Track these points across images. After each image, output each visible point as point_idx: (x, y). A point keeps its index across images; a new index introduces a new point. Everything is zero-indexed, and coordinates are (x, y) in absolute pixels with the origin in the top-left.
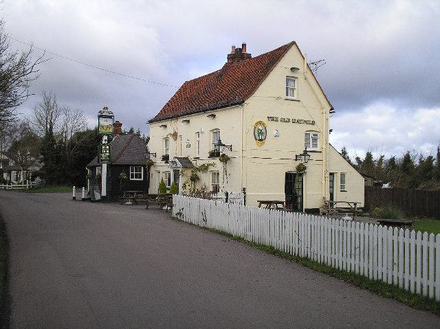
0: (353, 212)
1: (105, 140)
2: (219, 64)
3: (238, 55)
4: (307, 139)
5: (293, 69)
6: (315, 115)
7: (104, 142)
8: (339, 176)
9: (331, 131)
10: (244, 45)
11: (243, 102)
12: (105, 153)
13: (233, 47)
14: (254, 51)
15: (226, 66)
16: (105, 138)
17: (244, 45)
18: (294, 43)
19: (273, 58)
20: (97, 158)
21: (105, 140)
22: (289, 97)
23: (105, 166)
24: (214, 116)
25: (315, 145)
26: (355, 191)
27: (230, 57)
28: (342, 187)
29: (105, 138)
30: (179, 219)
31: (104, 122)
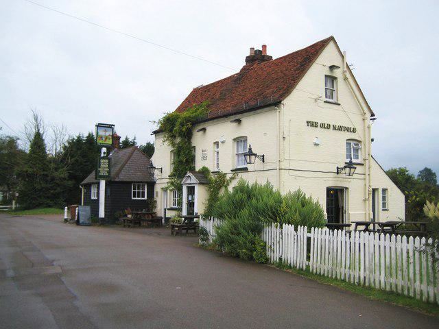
0: (392, 229)
1: (104, 153)
2: (235, 65)
3: (257, 58)
4: (349, 150)
5: (332, 68)
6: (353, 120)
7: (102, 155)
8: (380, 191)
9: (372, 140)
10: (264, 47)
11: (280, 102)
12: (104, 167)
13: (252, 49)
14: (275, 52)
15: (244, 69)
16: (104, 150)
17: (264, 47)
18: (332, 39)
19: (304, 59)
20: (94, 173)
21: (104, 153)
22: (328, 100)
23: (103, 183)
24: (239, 121)
25: (357, 157)
26: (396, 207)
27: (248, 59)
28: (384, 205)
29: (104, 150)
30: (283, 267)
31: (101, 133)
